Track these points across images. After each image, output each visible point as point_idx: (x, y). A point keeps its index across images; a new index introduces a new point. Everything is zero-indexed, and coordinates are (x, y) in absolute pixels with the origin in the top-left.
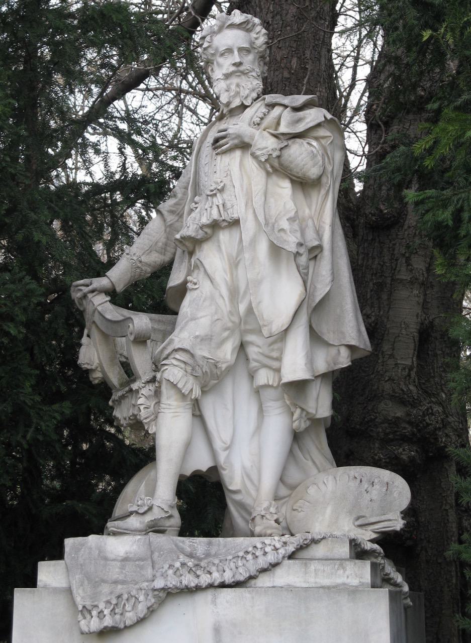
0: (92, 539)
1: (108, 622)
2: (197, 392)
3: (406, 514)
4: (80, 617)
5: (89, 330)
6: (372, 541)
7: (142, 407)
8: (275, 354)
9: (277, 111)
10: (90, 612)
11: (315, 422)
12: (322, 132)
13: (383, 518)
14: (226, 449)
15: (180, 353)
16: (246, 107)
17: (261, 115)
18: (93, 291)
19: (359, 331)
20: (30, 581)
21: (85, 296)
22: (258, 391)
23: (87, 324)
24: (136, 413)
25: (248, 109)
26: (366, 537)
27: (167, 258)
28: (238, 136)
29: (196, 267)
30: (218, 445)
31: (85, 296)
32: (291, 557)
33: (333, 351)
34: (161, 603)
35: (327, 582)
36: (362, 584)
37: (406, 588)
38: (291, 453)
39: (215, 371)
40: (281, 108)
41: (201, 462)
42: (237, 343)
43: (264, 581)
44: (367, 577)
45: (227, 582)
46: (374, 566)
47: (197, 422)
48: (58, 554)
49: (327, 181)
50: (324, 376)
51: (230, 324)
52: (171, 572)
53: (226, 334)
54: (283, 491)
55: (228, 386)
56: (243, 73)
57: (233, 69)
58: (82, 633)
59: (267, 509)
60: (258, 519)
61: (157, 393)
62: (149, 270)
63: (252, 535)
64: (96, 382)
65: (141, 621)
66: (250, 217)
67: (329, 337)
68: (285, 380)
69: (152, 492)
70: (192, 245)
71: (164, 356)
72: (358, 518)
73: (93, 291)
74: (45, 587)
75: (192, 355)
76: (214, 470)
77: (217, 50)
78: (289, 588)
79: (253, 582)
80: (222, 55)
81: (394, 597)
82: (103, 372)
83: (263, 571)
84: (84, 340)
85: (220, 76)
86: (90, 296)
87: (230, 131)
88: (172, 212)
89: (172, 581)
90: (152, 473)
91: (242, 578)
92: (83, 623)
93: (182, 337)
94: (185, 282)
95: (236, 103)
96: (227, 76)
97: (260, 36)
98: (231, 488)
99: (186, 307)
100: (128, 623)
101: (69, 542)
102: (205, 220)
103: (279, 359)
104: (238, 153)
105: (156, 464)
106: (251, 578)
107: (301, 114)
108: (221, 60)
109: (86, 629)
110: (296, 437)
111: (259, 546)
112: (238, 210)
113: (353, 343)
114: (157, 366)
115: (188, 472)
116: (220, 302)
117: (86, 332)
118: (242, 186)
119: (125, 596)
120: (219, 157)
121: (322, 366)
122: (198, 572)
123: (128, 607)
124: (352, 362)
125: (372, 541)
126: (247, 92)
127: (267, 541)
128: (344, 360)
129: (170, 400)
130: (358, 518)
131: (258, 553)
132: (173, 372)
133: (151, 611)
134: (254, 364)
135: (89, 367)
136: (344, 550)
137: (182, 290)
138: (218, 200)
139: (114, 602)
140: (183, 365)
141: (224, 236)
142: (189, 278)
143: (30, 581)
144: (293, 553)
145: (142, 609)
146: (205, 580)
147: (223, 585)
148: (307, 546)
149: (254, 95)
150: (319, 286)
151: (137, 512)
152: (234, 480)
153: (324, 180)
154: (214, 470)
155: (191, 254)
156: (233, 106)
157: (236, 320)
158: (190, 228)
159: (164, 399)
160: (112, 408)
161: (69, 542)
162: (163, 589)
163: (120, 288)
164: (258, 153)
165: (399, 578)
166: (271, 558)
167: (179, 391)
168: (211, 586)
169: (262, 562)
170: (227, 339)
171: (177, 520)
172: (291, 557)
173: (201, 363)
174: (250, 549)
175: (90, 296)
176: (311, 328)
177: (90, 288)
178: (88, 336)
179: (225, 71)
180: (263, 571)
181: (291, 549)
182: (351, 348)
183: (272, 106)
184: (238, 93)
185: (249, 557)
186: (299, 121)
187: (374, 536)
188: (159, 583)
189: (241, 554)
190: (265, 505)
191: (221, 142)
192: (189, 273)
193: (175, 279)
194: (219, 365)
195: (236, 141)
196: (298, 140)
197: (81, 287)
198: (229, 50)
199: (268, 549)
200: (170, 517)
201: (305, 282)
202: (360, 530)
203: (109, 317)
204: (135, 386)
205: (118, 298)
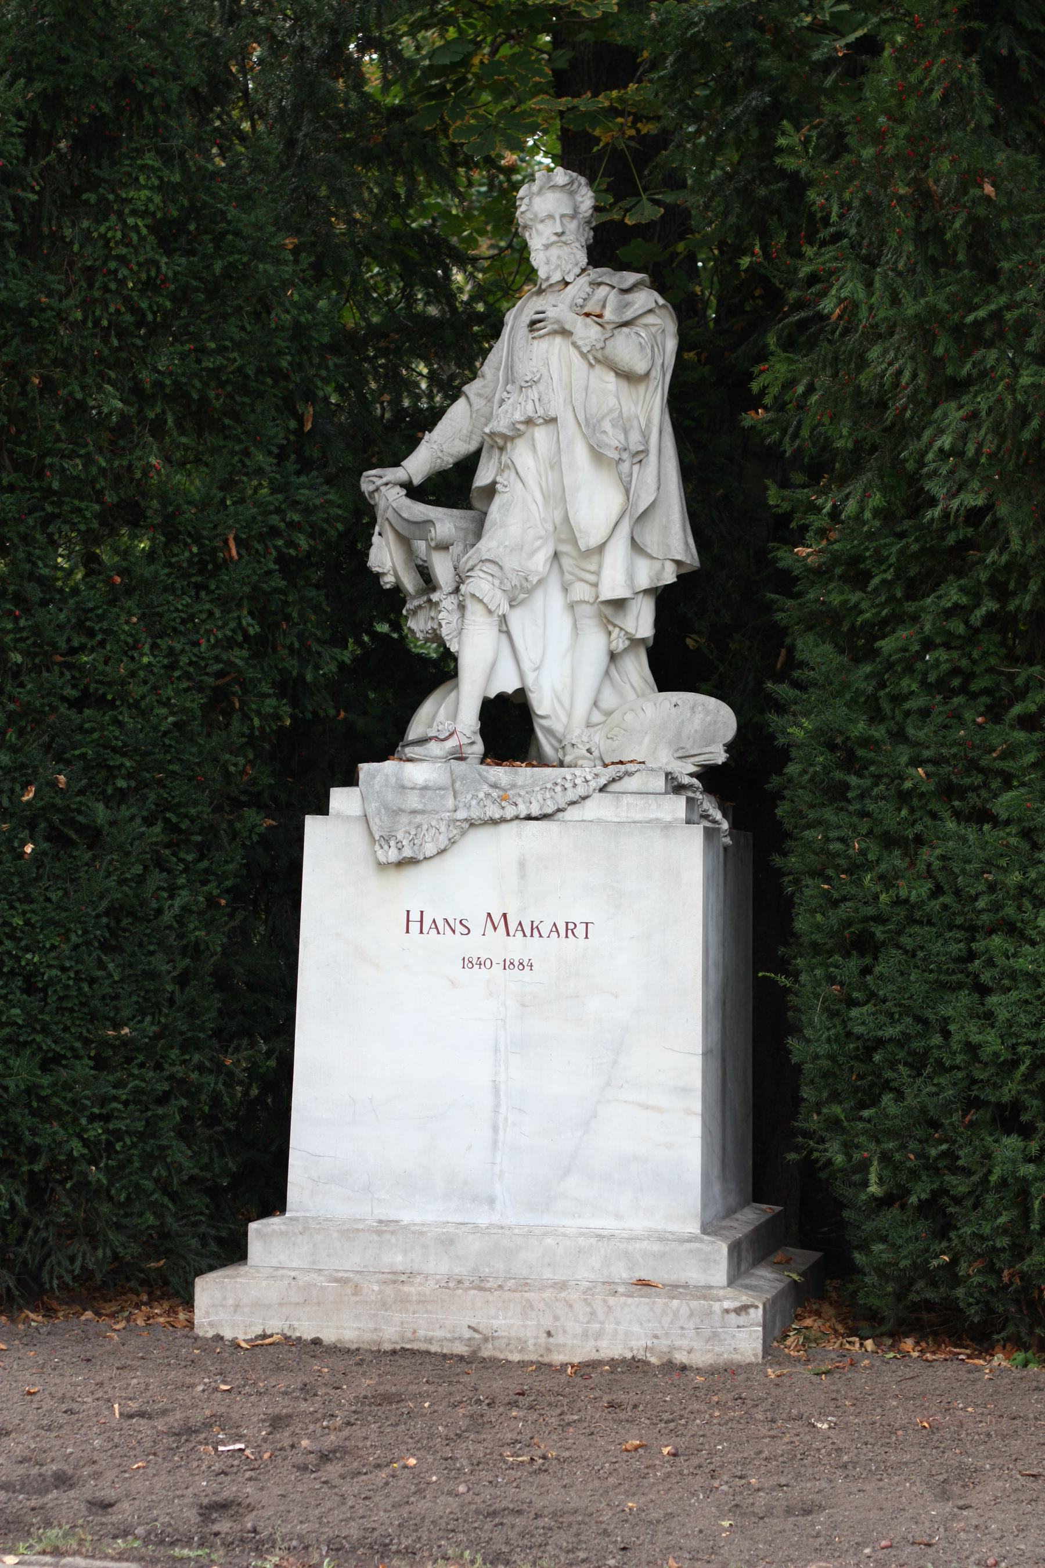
0: (387, 763)
1: (407, 853)
2: (505, 607)
3: (729, 747)
4: (377, 847)
5: (381, 527)
6: (691, 775)
7: (443, 623)
8: (593, 567)
9: (603, 291)
10: (387, 842)
11: (635, 642)
12: (650, 319)
13: (705, 750)
14: (537, 669)
15: (488, 564)
16: (567, 284)
17: (584, 296)
18: (387, 484)
19: (687, 544)
20: (322, 809)
21: (377, 490)
22: (572, 606)
23: (379, 520)
24: (436, 626)
25: (570, 287)
26: (684, 770)
27: (472, 447)
28: (558, 322)
29: (507, 466)
30: (526, 665)
31: (377, 490)
32: (602, 790)
33: (657, 565)
34: (463, 833)
35: (639, 817)
36: (676, 820)
37: (725, 826)
38: (607, 673)
39: (525, 584)
40: (607, 288)
41: (508, 685)
42: (551, 552)
43: (572, 813)
44: (681, 813)
45: (534, 814)
46: (690, 801)
47: (504, 637)
48: (351, 780)
49: (656, 373)
50: (646, 592)
51: (543, 533)
52: (474, 802)
53: (539, 543)
54: (597, 717)
55: (539, 596)
56: (565, 243)
57: (555, 238)
58: (380, 864)
59: (580, 736)
60: (569, 748)
61: (462, 607)
62: (451, 460)
63: (561, 764)
64: (388, 586)
65: (442, 852)
66: (570, 416)
67: (652, 549)
68: (602, 598)
69: (454, 716)
70: (501, 442)
71: (468, 566)
72: (677, 750)
73: (387, 484)
74: (338, 815)
75: (501, 567)
76: (521, 692)
77: (536, 216)
78: (599, 822)
79: (560, 815)
80: (542, 221)
81: (710, 834)
82: (396, 575)
83: (572, 803)
84: (376, 539)
85: (540, 246)
86: (383, 489)
87: (549, 314)
88: (479, 395)
89: (475, 813)
90: (453, 695)
91: (549, 811)
92: (380, 853)
93: (488, 545)
94: (494, 483)
95: (556, 277)
96: (547, 247)
97: (586, 199)
98: (539, 712)
99: (495, 509)
100: (428, 854)
101: (365, 769)
102: (518, 416)
103: (598, 573)
104: (558, 340)
105: (457, 686)
106: (559, 810)
107: (629, 297)
108: (540, 227)
109: (383, 859)
110: (613, 657)
111: (569, 777)
112: (557, 406)
113: (678, 557)
114: (460, 579)
115: (492, 695)
116: (533, 507)
117: (377, 529)
118: (560, 379)
119: (425, 827)
120: (536, 342)
121: (644, 581)
122: (504, 804)
123: (428, 838)
124: (678, 577)
125: (691, 775)
126: (570, 266)
127: (578, 772)
128: (669, 577)
129: (475, 614)
130: (677, 750)
131: (568, 785)
132: (480, 584)
133: (452, 842)
134: (568, 577)
135: (380, 570)
136: (660, 784)
137: (490, 491)
138: (533, 394)
139: (413, 832)
140: (490, 578)
141: (541, 435)
142: (499, 479)
143: (322, 809)
144: (605, 786)
145: (443, 841)
146: (510, 812)
147: (529, 818)
148: (620, 778)
149: (578, 271)
150: (643, 495)
151: (436, 738)
152: (542, 703)
153: (653, 374)
154: (521, 692)
155: (502, 449)
156: (553, 281)
157: (551, 529)
158: (501, 424)
159: (468, 614)
160: (406, 618)
161: (365, 769)
162: (466, 820)
163: (417, 481)
164: (580, 343)
165: (718, 815)
166: (581, 791)
167: (486, 606)
168: (517, 818)
169: (572, 795)
170: (539, 548)
171: (479, 748)
172: (602, 790)
173: (509, 575)
174: (559, 781)
175: (383, 489)
176: (633, 539)
177: (384, 480)
178: (380, 534)
179: (545, 242)
180: (572, 803)
181: (603, 781)
182: (678, 563)
183: (596, 284)
184: (558, 266)
185: (558, 789)
186: (627, 305)
187: (693, 769)
188: (462, 814)
189: (549, 785)
190: (577, 732)
191: (538, 325)
192: (501, 471)
193: (483, 478)
194: (530, 578)
195: (556, 327)
196: (625, 330)
197: (373, 481)
198: (551, 217)
199: (578, 781)
200: (473, 743)
201: (627, 491)
202: (679, 763)
203: (405, 515)
204: (435, 597)
205: (415, 492)
